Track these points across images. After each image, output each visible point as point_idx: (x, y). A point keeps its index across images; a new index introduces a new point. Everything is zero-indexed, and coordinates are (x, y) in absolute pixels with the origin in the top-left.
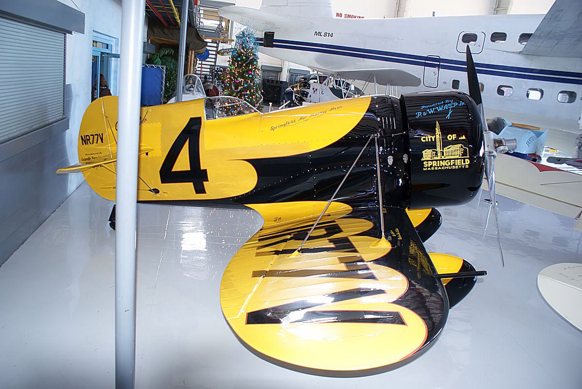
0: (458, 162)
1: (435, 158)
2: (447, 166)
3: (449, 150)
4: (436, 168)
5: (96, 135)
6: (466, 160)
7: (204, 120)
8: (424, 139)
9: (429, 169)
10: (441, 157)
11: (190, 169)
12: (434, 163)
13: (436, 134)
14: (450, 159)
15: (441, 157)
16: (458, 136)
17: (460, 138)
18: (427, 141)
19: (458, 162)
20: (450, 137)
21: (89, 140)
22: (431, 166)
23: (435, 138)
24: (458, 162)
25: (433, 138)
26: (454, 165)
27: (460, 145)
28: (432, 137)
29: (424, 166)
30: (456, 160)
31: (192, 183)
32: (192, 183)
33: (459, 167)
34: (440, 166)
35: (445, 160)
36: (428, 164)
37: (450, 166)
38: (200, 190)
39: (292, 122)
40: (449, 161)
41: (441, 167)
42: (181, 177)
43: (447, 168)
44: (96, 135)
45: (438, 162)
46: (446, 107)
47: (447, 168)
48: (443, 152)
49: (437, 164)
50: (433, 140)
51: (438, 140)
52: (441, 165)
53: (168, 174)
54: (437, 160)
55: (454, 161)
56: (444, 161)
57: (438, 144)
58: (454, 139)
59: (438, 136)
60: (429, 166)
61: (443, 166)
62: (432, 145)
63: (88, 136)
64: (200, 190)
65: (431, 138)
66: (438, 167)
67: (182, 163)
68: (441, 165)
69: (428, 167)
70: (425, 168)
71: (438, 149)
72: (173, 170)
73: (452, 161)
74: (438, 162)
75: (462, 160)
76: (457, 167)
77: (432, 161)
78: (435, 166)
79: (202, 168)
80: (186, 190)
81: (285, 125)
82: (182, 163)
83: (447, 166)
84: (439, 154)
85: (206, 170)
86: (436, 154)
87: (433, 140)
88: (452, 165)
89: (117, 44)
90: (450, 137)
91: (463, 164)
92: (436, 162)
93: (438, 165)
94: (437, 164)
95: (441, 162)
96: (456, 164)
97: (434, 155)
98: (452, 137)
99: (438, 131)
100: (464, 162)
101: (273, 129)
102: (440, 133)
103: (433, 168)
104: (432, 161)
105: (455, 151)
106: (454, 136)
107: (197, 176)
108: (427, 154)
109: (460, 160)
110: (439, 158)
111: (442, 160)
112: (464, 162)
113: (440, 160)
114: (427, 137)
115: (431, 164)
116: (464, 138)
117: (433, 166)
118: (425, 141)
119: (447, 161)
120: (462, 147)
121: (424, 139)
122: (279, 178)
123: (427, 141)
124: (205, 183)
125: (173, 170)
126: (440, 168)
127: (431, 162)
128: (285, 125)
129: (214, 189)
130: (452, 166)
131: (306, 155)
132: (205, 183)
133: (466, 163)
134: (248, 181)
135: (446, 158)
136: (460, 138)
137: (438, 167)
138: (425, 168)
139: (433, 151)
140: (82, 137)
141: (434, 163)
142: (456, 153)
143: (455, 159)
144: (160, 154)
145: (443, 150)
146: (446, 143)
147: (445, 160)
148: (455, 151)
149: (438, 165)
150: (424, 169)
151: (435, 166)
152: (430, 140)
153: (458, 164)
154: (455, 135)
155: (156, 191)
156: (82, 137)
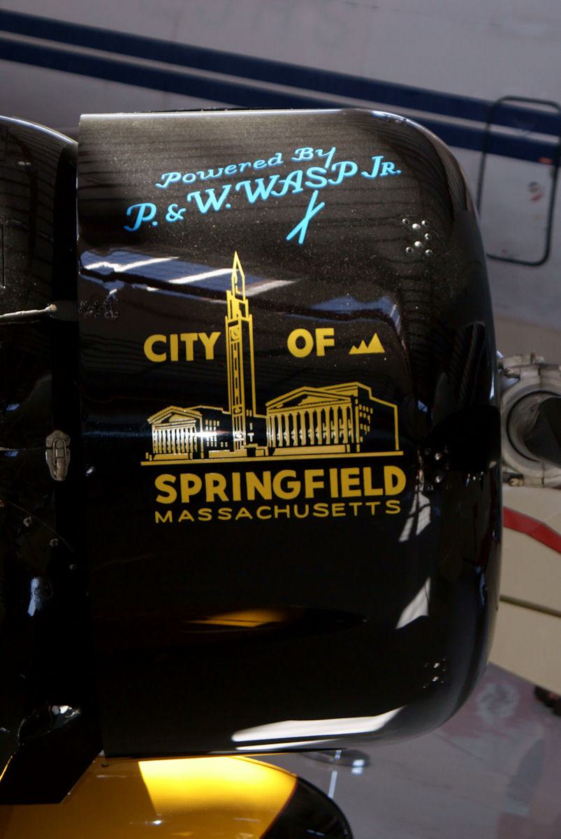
4: (225, 514)
9: (186, 515)
15: (251, 452)
23: (220, 346)
25: (209, 342)
28: (203, 336)
29: (160, 499)
36: (177, 486)
37: (301, 500)
40: (293, 473)
41: (252, 506)
49: (229, 491)
52: (251, 496)
58: (321, 352)
65: (199, 346)
66: (235, 507)
68: (251, 496)
69: (177, 507)
70: (163, 509)
75: (367, 472)
78: (218, 503)
87: (210, 355)
88: (309, 494)
90: (301, 343)
91: (369, 491)
96: (334, 494)
102: (249, 318)
103: (205, 514)
104: (201, 470)
110: (240, 454)
114: (174, 338)
117: (210, 498)
133: (390, 490)
135: (281, 454)
136: (354, 351)
145: (262, 410)
149: (237, 496)
152: (190, 356)
154: (330, 331)
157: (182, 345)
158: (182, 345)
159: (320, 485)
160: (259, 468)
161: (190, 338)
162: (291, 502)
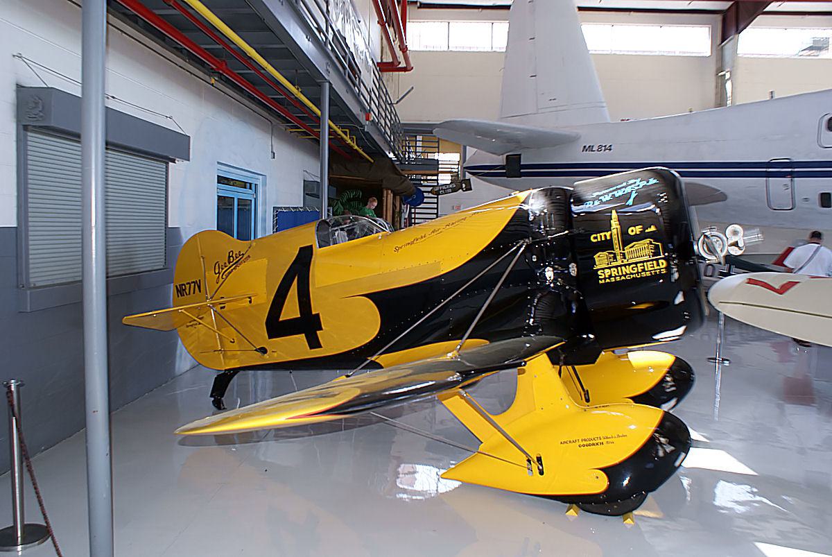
0: (648, 266)
1: (614, 264)
2: (632, 274)
3: (632, 249)
4: (618, 279)
5: (192, 282)
6: (660, 261)
7: (317, 250)
8: (595, 238)
9: (608, 280)
10: (622, 262)
11: (299, 316)
12: (614, 272)
13: (612, 228)
14: (636, 263)
15: (622, 262)
16: (645, 228)
17: (646, 231)
18: (599, 240)
19: (648, 266)
20: (632, 231)
21: (184, 290)
22: (610, 276)
23: (611, 235)
24: (649, 266)
25: (608, 234)
26: (644, 270)
27: (648, 241)
28: (606, 233)
29: (600, 277)
30: (645, 264)
31: (304, 335)
32: (304, 335)
33: (651, 273)
34: (623, 275)
35: (629, 265)
37: (638, 273)
38: (314, 343)
39: (422, 237)
40: (634, 265)
41: (625, 276)
42: (290, 328)
43: (634, 276)
44: (192, 282)
45: (619, 268)
46: (628, 190)
47: (634, 276)
48: (624, 254)
49: (618, 273)
50: (608, 238)
51: (615, 237)
53: (276, 327)
54: (616, 267)
55: (642, 264)
56: (627, 267)
57: (615, 241)
59: (614, 231)
60: (607, 276)
61: (627, 274)
62: (607, 245)
63: (184, 284)
64: (314, 343)
65: (605, 236)
66: (620, 276)
67: (291, 310)
68: (624, 273)
69: (605, 279)
70: (601, 279)
71: (617, 251)
72: (281, 319)
73: (639, 265)
74: (619, 268)
76: (648, 274)
77: (610, 268)
79: (313, 313)
80: (295, 347)
81: (412, 243)
82: (291, 310)
83: (632, 274)
84: (618, 257)
85: (318, 315)
86: (615, 258)
87: (608, 238)
88: (640, 271)
89: (265, 184)
91: (656, 268)
92: (615, 269)
93: (620, 274)
94: (618, 273)
95: (623, 268)
97: (612, 260)
98: (635, 230)
99: (615, 224)
100: (658, 265)
101: (397, 250)
102: (619, 227)
104: (610, 268)
105: (643, 249)
106: (638, 229)
107: (309, 325)
108: (601, 259)
109: (651, 262)
110: (619, 263)
111: (625, 265)
112: (658, 265)
113: (621, 266)
115: (609, 274)
116: (653, 229)
117: (613, 275)
118: (596, 240)
119: (632, 266)
120: (651, 243)
121: (595, 238)
122: (408, 313)
123: (599, 240)
124: (318, 332)
125: (281, 319)
126: (623, 278)
127: (608, 270)
128: (412, 243)
129: (334, 341)
130: (640, 273)
131: (437, 280)
132: (318, 332)
134: (368, 324)
135: (630, 261)
136: (646, 231)
137: (620, 276)
138: (601, 279)
139: (610, 253)
140: (176, 286)
141: (614, 272)
142: (643, 252)
143: (643, 262)
144: (265, 299)
145: (624, 250)
146: (627, 240)
147: (629, 265)
148: (643, 249)
150: (600, 282)
151: (616, 276)
152: (603, 239)
153: (650, 269)
155: (263, 350)
156: (176, 286)
157: (601, 236)
158: (601, 236)
159: (643, 268)
160: (625, 265)
161: (602, 234)
162: (635, 273)
